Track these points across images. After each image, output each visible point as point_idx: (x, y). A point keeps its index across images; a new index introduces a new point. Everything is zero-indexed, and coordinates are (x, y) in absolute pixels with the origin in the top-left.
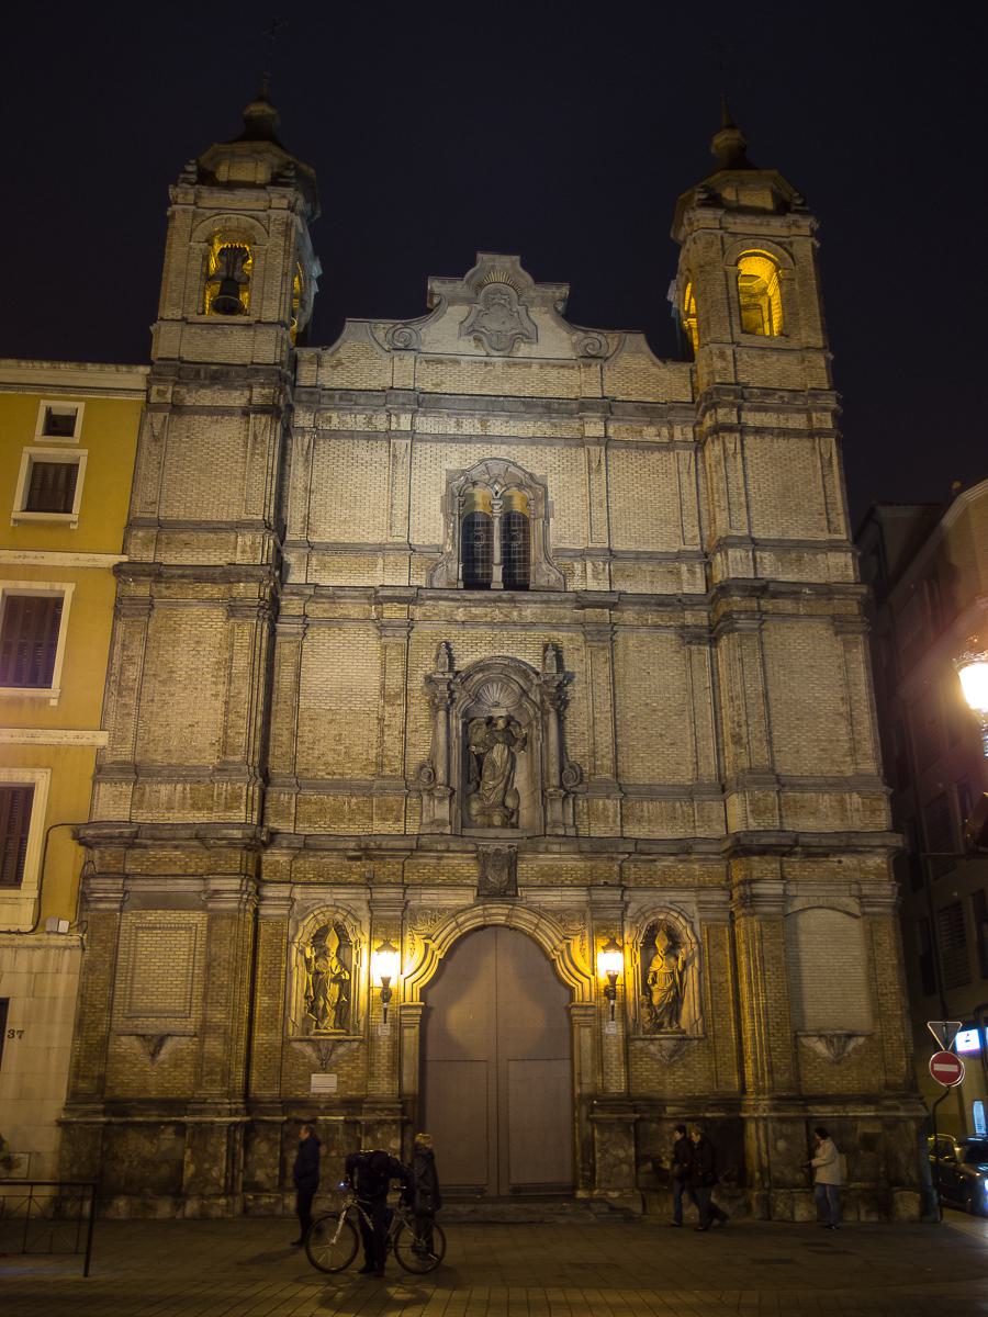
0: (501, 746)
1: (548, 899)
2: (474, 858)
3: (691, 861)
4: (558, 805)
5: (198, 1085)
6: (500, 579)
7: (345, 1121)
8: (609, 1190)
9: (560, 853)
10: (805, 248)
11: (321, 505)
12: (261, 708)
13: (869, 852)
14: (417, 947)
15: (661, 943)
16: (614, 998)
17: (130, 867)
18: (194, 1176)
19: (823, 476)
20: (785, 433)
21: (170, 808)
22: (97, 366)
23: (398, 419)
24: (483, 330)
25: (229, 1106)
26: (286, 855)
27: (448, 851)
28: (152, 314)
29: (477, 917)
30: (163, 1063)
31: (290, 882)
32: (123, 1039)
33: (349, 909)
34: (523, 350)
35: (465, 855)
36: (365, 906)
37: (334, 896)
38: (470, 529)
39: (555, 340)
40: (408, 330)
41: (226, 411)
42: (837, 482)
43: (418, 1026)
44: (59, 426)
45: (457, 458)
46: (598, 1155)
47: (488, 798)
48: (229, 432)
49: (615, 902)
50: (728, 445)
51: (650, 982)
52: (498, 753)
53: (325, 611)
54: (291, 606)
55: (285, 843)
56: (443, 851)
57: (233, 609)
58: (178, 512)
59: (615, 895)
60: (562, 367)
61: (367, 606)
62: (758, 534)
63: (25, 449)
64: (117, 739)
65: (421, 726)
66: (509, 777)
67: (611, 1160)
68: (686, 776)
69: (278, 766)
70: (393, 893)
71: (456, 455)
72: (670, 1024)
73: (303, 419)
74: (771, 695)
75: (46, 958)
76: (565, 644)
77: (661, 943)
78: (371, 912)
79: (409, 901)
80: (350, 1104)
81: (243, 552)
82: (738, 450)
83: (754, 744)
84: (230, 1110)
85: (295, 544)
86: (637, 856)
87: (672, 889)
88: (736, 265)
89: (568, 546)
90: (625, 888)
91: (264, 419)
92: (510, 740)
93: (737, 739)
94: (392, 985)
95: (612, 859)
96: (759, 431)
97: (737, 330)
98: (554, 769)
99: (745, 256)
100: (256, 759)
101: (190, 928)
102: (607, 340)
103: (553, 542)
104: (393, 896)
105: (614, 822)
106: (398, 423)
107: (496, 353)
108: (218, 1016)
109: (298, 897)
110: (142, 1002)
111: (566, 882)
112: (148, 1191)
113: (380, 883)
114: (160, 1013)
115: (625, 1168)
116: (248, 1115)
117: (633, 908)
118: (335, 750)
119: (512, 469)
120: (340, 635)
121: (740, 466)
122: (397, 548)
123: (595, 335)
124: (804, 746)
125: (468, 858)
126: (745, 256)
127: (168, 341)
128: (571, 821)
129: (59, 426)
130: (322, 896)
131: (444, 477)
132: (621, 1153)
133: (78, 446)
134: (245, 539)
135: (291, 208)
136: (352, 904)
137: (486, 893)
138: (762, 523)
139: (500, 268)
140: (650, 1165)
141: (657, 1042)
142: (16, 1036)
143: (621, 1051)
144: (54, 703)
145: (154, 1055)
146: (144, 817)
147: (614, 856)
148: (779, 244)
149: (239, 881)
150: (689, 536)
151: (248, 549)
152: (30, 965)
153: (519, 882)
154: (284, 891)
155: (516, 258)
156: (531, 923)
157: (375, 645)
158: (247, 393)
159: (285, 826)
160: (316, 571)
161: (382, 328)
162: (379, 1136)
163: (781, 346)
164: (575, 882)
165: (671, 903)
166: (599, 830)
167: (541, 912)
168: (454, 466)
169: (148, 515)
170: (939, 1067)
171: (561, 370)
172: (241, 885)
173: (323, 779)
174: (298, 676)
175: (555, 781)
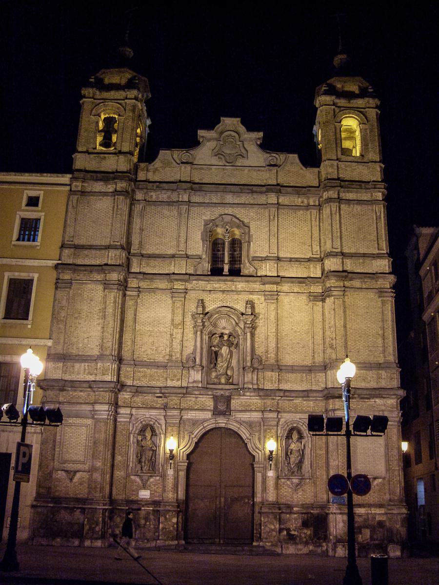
1: (244, 416)
2: (212, 398)
3: (309, 401)
4: (250, 375)
5: (89, 493)
6: (227, 271)
7: (153, 510)
8: (266, 542)
9: (250, 396)
10: (373, 113)
11: (147, 237)
12: (118, 330)
13: (388, 397)
14: (186, 436)
15: (295, 436)
16: (272, 460)
17: (61, 399)
19: (377, 223)
20: (359, 202)
22: (49, 175)
23: (182, 196)
24: (223, 153)
25: (103, 502)
26: (128, 395)
27: (200, 395)
28: (73, 149)
29: (212, 424)
30: (76, 483)
31: (130, 407)
32: (59, 472)
33: (156, 419)
34: (240, 162)
35: (208, 396)
36: (163, 418)
37: (150, 414)
38: (215, 246)
39: (257, 157)
40: (188, 154)
41: (105, 194)
42: (383, 225)
43: (185, 471)
44: (33, 202)
45: (208, 214)
46: (263, 527)
47: (219, 371)
49: (274, 418)
51: (289, 453)
52: (224, 350)
53: (148, 285)
54: (133, 283)
55: (128, 390)
56: (197, 395)
57: (106, 285)
58: (82, 241)
59: (274, 415)
60: (259, 170)
61: (167, 283)
62: (346, 250)
63: (18, 212)
64: (56, 343)
65: (190, 338)
66: (229, 361)
67: (267, 529)
68: (308, 362)
69: (126, 354)
70: (176, 413)
71: (209, 213)
73: (139, 196)
74: (348, 326)
76: (256, 301)
77: (295, 436)
78: (166, 420)
79: (182, 416)
80: (155, 503)
81: (112, 259)
82: (338, 211)
83: (339, 348)
84: (103, 503)
85: (134, 255)
86: (285, 398)
87: (301, 413)
88: (340, 122)
89: (258, 255)
90: (279, 412)
91: (121, 198)
92: (230, 344)
94: (174, 452)
95: (273, 399)
96: (348, 202)
97: (339, 153)
98: (249, 358)
99: (345, 117)
100: (116, 353)
101: (87, 426)
102: (281, 157)
103: (252, 254)
104: (175, 414)
105: (275, 383)
106: (182, 198)
107: (228, 164)
108: (99, 464)
109: (134, 413)
110: (67, 457)
111: (253, 409)
113: (170, 408)
114: (75, 462)
115: (274, 533)
116: (110, 506)
117: (282, 420)
118: (151, 349)
119: (234, 219)
121: (338, 218)
122: (181, 256)
123: (274, 155)
124: (361, 349)
125: (209, 398)
126: (343, 118)
127: (80, 161)
128: (256, 382)
129: (33, 202)
130: (145, 413)
131: (203, 223)
132: (273, 527)
133: (41, 211)
134: (112, 253)
135: (136, 99)
136: (157, 417)
137: (216, 413)
138: (347, 245)
139: (230, 123)
140: (285, 532)
141: (290, 480)
144: (29, 326)
145: (71, 480)
146: (67, 377)
147: (274, 398)
148: (361, 112)
149: (108, 406)
150: (315, 250)
151: (114, 257)
153: (232, 409)
154: (128, 411)
155: (239, 119)
156: (237, 427)
158: (114, 186)
159: (129, 382)
160: (144, 267)
161: (178, 154)
162: (168, 516)
163: (362, 160)
164: (257, 409)
165: (300, 419)
166: (268, 386)
167: (240, 423)
168: (208, 218)
169: (70, 242)
171: (258, 172)
172: (109, 408)
173: (146, 361)
174: (135, 315)
175: (249, 364)
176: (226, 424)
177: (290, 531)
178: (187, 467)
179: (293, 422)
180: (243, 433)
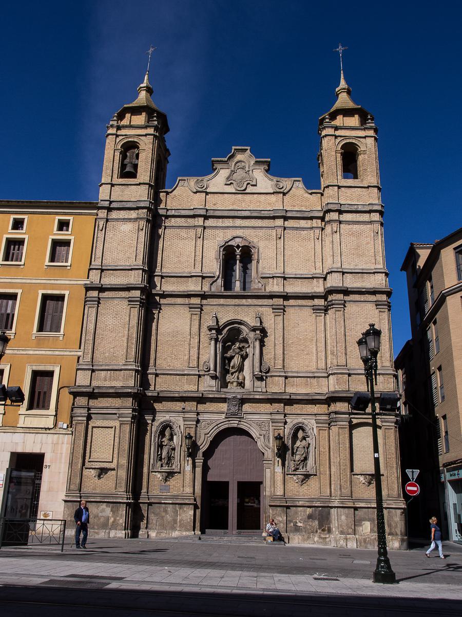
0: (237, 355)
18: (113, 522)
21: (105, 380)
44: (63, 225)
48: (128, 227)
50: (334, 228)
62: (347, 267)
71: (221, 234)
72: (303, 467)
75: (58, 437)
83: (339, 354)
93: (332, 353)
102: (286, 183)
112: (96, 527)
120: (173, 310)
130: (165, 415)
132: (281, 519)
140: (292, 524)
142: (48, 467)
143: (282, 479)
144: (61, 338)
152: (53, 441)
157: (189, 315)
170: (415, 489)
176: (238, 424)
177: (297, 523)
178: (203, 463)
179: (300, 423)
180: (254, 433)
